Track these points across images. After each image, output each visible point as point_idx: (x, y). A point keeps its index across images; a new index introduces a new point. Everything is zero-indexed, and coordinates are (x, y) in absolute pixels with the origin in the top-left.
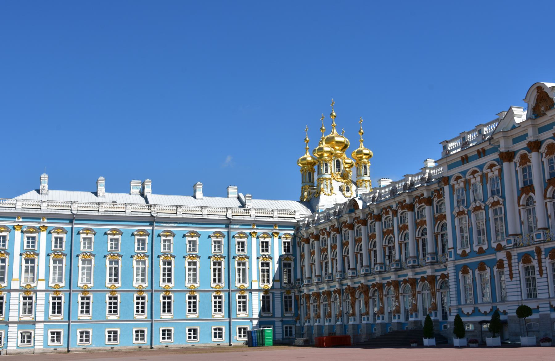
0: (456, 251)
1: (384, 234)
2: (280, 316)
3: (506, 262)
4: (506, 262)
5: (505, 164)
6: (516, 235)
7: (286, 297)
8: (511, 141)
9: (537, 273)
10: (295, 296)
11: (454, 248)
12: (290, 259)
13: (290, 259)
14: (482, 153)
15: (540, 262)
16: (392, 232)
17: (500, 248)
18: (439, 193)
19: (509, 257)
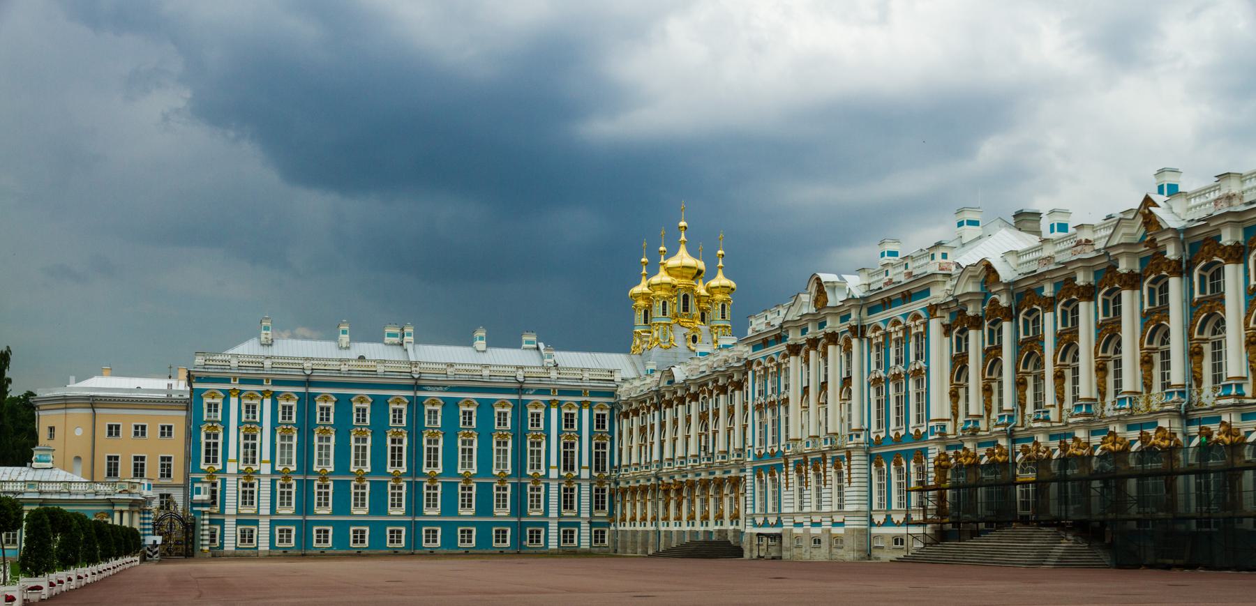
7: (597, 490)
11: (753, 446)
12: (604, 438)
13: (604, 438)
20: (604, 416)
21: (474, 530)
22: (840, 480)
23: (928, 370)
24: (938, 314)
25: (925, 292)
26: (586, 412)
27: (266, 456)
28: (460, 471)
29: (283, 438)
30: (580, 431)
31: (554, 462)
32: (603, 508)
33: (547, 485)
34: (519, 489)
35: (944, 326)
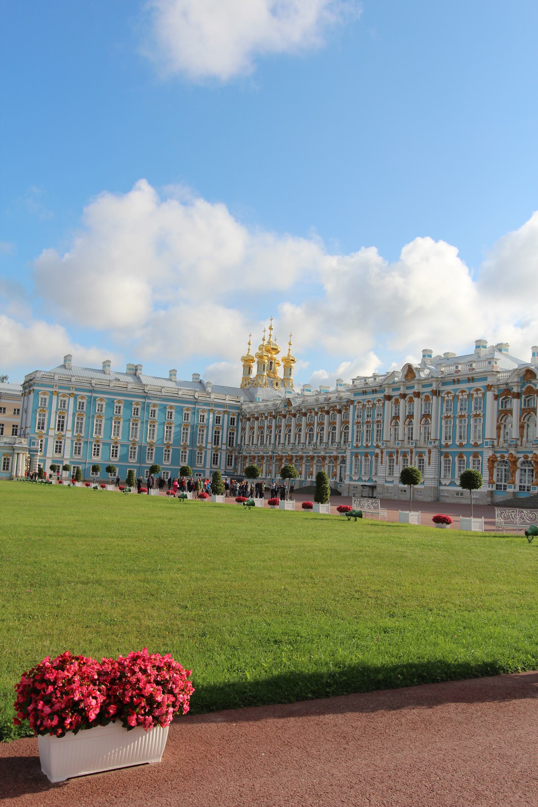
0: (352, 444)
1: (307, 425)
2: (224, 468)
3: (380, 455)
4: (380, 455)
5: (386, 402)
6: (387, 441)
8: (391, 389)
9: (395, 463)
10: (235, 456)
11: (352, 442)
12: (233, 430)
13: (233, 430)
14: (374, 392)
15: (397, 458)
16: (313, 425)
17: (378, 447)
18: (347, 407)
19: (382, 453)
20: (234, 419)
21: (170, 472)
22: (377, 462)
23: (484, 415)
24: (492, 389)
25: (485, 379)
26: (226, 416)
27: (70, 427)
28: (182, 444)
29: (78, 419)
30: (223, 426)
31: (210, 440)
32: (231, 465)
33: (206, 452)
34: (192, 452)
35: (494, 395)
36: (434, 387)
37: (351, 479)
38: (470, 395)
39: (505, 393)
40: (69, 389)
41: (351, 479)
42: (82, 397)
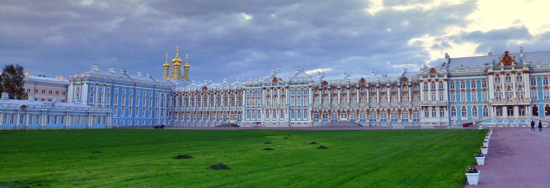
17: (259, 107)
34: (153, 111)
36: (287, 85)
37: (245, 120)
38: (302, 89)
39: (316, 89)
40: (103, 82)
41: (245, 120)
42: (109, 86)
